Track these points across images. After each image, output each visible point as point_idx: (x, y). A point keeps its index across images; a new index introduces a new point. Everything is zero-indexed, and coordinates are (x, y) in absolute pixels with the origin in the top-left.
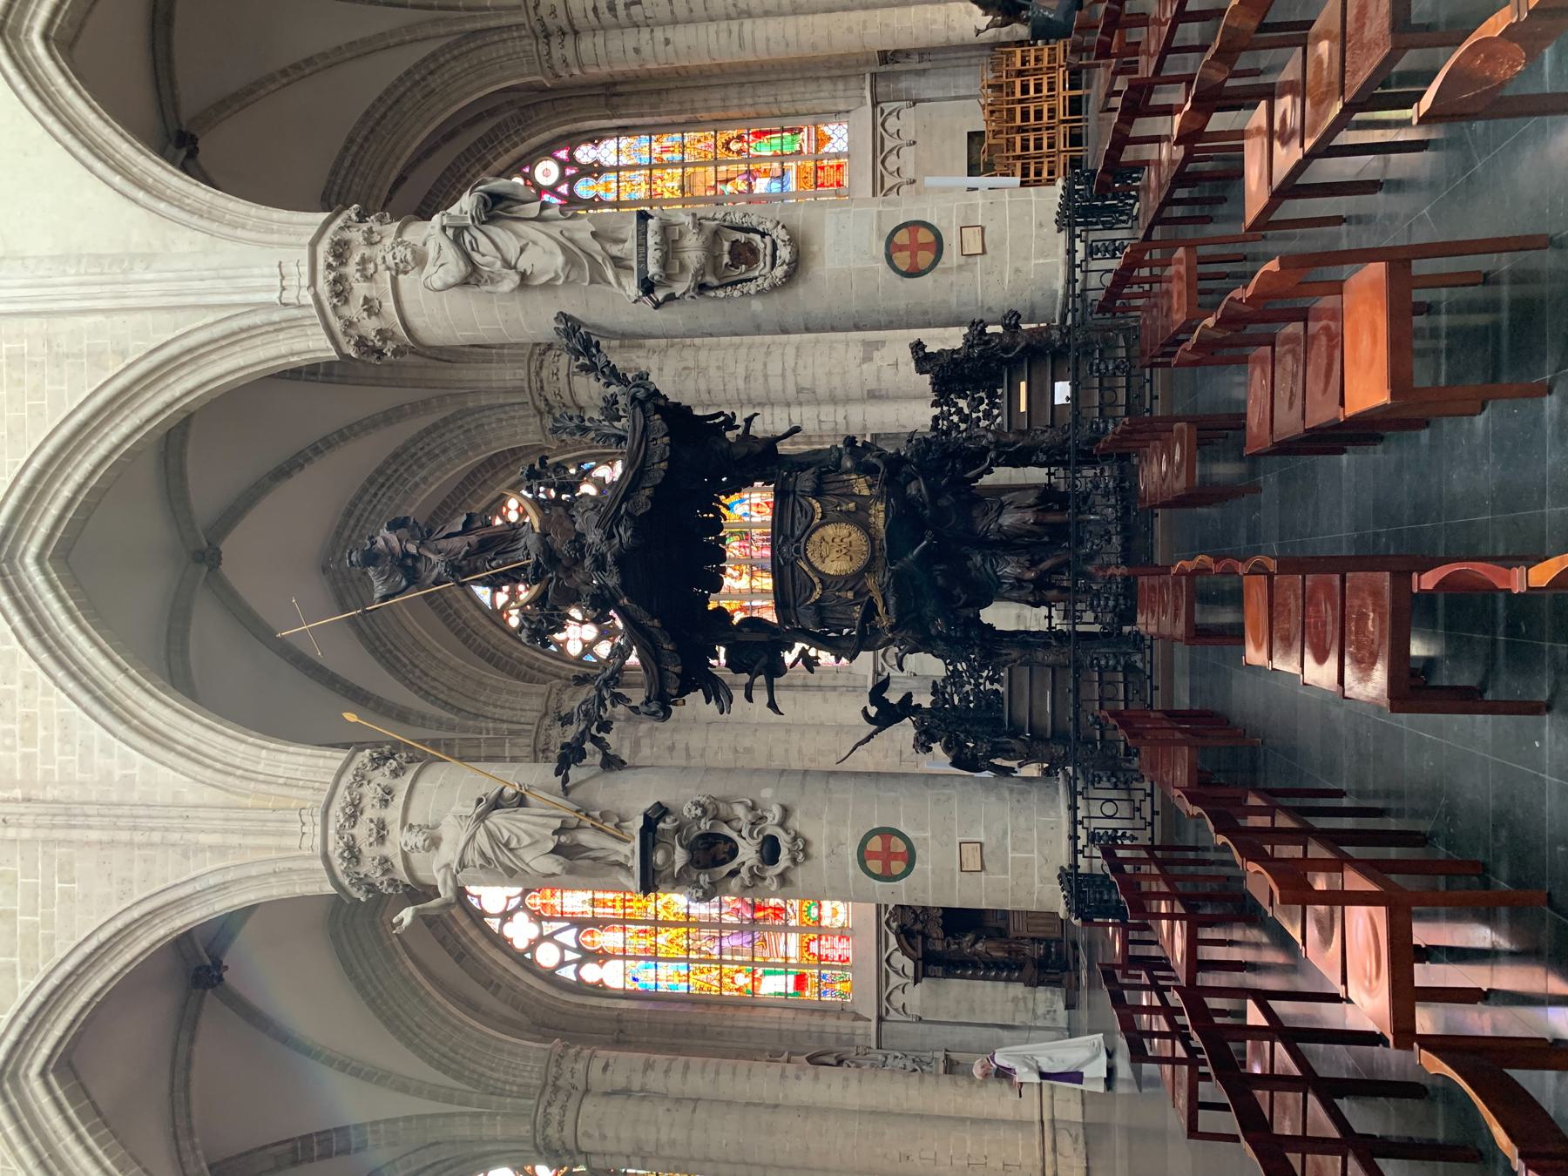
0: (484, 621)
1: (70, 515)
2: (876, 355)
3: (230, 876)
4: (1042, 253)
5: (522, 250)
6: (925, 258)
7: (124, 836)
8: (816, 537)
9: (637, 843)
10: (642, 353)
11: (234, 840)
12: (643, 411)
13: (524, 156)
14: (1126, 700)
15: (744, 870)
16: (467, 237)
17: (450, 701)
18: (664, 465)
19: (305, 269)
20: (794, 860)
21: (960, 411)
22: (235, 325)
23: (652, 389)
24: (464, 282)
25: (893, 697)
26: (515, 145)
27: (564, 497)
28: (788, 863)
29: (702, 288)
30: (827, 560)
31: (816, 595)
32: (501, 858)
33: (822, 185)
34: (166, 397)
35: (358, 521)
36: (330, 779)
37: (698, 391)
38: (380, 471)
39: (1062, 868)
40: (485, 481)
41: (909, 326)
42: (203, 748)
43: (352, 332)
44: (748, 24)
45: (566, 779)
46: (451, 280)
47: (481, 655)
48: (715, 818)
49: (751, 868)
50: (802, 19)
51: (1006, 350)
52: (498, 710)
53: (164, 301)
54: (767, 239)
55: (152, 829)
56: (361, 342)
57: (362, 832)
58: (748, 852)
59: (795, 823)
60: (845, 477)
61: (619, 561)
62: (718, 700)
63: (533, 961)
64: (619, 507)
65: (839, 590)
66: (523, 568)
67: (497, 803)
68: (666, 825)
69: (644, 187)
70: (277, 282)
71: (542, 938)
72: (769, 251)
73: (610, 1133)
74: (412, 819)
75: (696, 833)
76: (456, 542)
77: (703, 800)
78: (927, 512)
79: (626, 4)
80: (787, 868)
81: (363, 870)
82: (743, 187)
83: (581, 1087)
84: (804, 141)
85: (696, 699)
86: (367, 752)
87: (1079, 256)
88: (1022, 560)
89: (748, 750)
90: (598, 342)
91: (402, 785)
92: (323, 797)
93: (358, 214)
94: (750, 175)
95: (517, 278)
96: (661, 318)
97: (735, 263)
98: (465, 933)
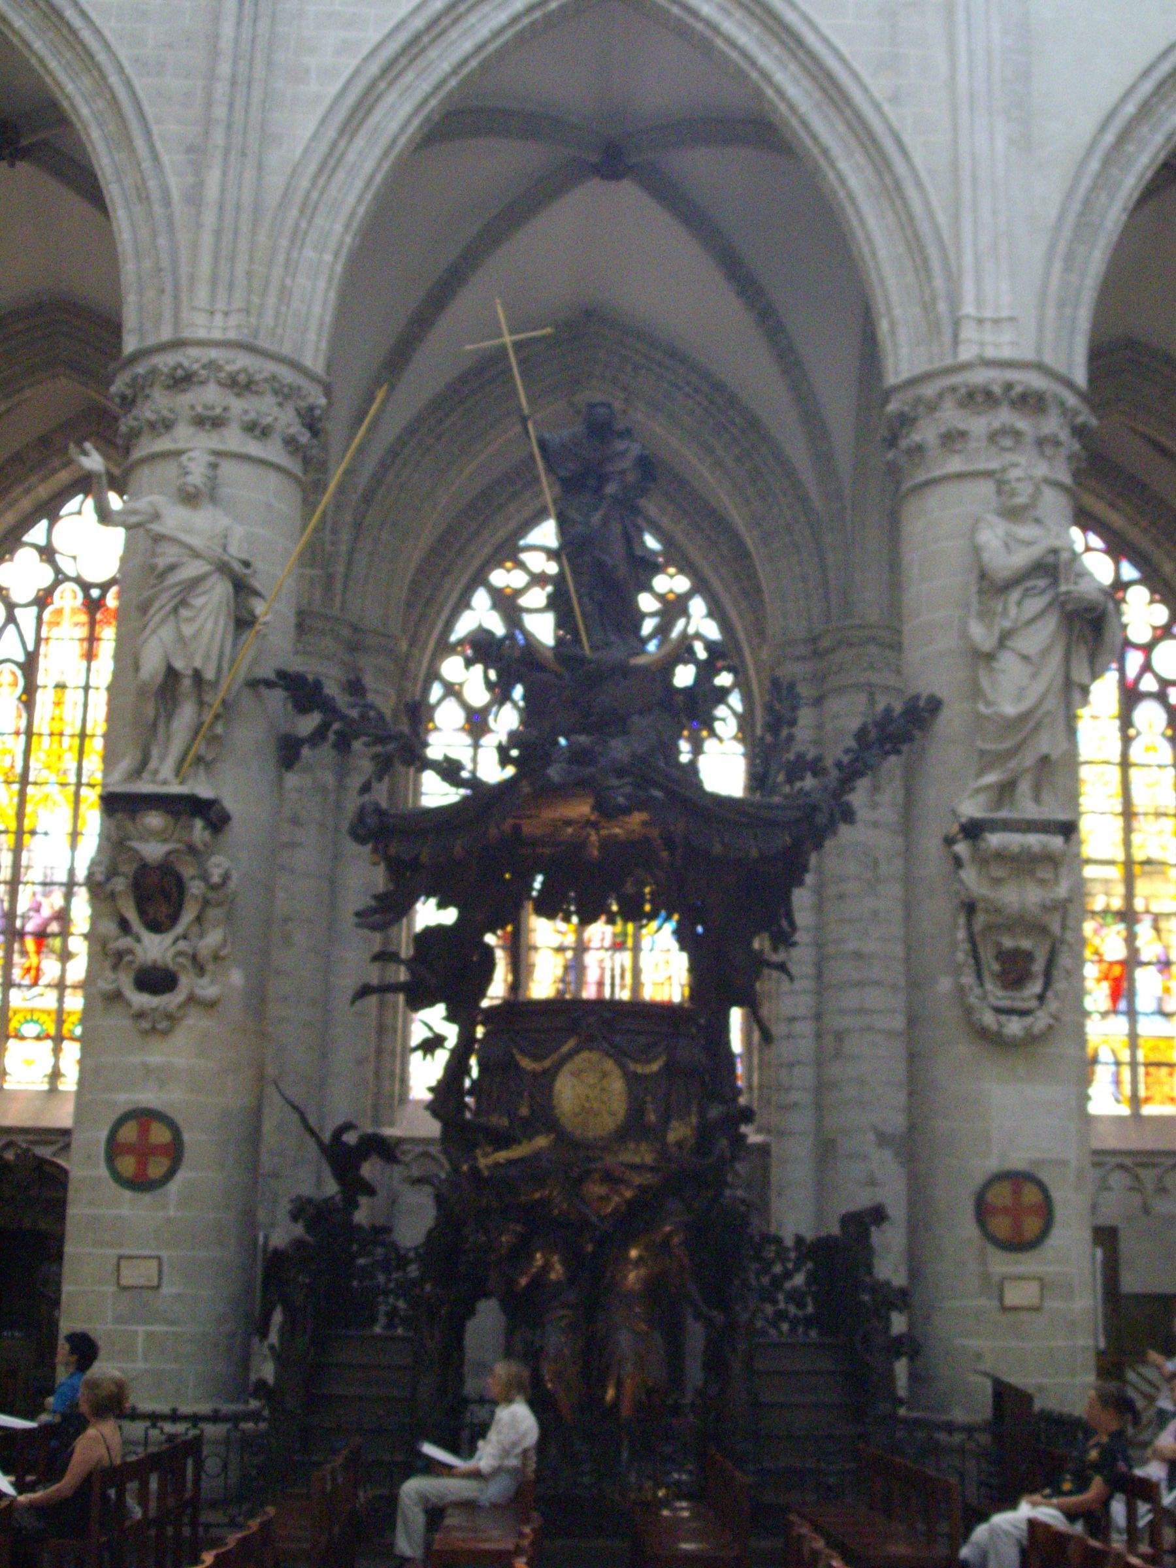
0: (501, 534)
2: (887, 1154)
3: (158, 209)
5: (1025, 658)
7: (224, 69)
8: (609, 1065)
9: (175, 789)
11: (209, 218)
19: (1006, 353)
20: (140, 1015)
21: (788, 1275)
24: (983, 576)
25: (369, 1169)
29: (970, 908)
30: (575, 1081)
31: (526, 1063)
32: (164, 598)
33: (1147, 1074)
34: (836, 150)
35: (660, 364)
36: (286, 350)
38: (733, 400)
41: (912, 1203)
42: (341, 175)
45: (269, 684)
46: (986, 556)
53: (965, 162)
55: (231, 106)
56: (905, 421)
57: (210, 395)
62: (372, 911)
64: (656, 784)
65: (531, 1096)
67: (242, 588)
68: (199, 831)
70: (988, 313)
71: (10, 607)
74: (228, 468)
75: (188, 871)
76: (619, 548)
77: (232, 885)
80: (128, 1004)
86: (323, 401)
89: (287, 940)
90: (898, 752)
91: (273, 451)
92: (263, 343)
96: (931, 845)
98: (27, 491)
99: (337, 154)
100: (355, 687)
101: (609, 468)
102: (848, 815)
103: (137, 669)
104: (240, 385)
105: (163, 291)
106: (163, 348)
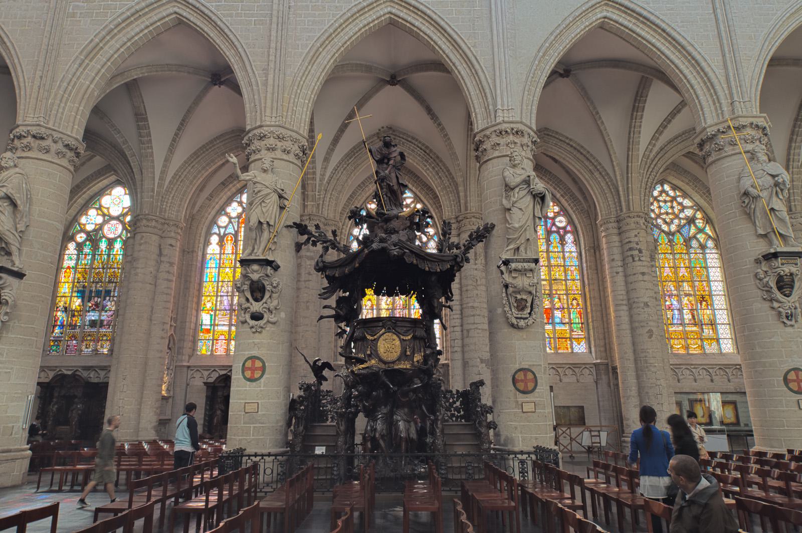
1: (408, 25)
2: (484, 365)
3: (255, 87)
4: (524, 439)
6: (521, 386)
8: (395, 337)
9: (262, 257)
14: (318, 479)
15: (248, 305)
16: (525, 186)
18: (427, 269)
20: (252, 327)
21: (454, 402)
22: (487, 91)
23: (461, 265)
24: (506, 185)
25: (326, 373)
26: (572, 208)
28: (251, 325)
29: (506, 286)
31: (369, 337)
37: (467, 286)
39: (245, 450)
43: (485, 139)
44: (625, 308)
45: (291, 227)
46: (507, 179)
47: (353, 193)
48: (272, 292)
49: (249, 308)
50: (628, 332)
51: (480, 423)
52: (328, 199)
54: (528, 316)
56: (481, 142)
57: (271, 141)
58: (256, 307)
59: (269, 327)
60: (422, 350)
61: (384, 250)
62: (324, 293)
63: (221, 215)
64: (408, 249)
69: (556, 263)
71: (230, 218)
72: (525, 316)
73: (142, 247)
75: (266, 283)
76: (395, 181)
77: (280, 287)
81: (255, 142)
82: (557, 306)
83: (163, 235)
84: (578, 333)
85: (326, 283)
87: (519, 456)
88: (384, 431)
89: (308, 308)
91: (291, 157)
92: (287, 126)
93: (535, 141)
94: (562, 309)
95: (508, 207)
97: (517, 300)
99: (308, 70)
101: (391, 156)
102: (467, 260)
104: (280, 138)
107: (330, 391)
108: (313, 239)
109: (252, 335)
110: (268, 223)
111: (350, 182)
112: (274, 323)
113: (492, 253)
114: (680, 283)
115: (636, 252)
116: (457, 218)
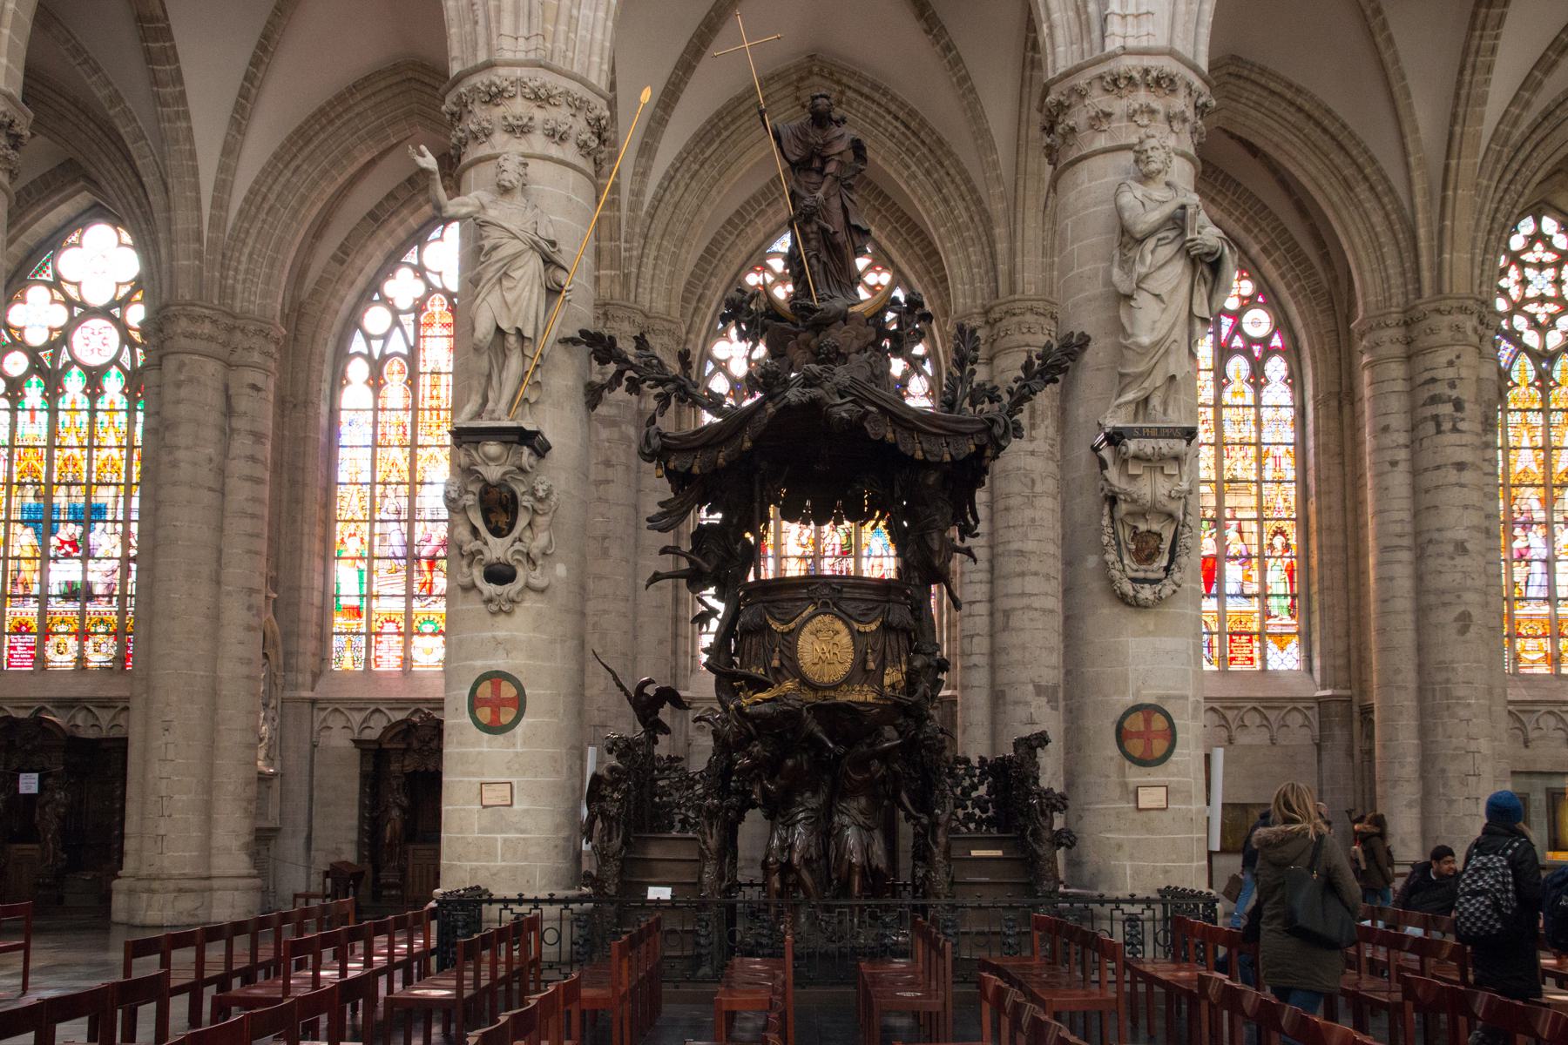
0: (752, 245)
8: (839, 625)
10: (1051, 431)
12: (980, 432)
13: (1276, 296)
17: (662, 205)
18: (919, 455)
23: (1003, 443)
26: (1289, 286)
27: (887, 343)
30: (813, 637)
31: (775, 626)
40: (912, 247)
47: (714, 241)
52: (651, 262)
60: (904, 658)
61: (815, 404)
64: (873, 404)
65: (781, 651)
66: (809, 295)
78: (865, 749)
79: (1437, 416)
88: (812, 850)
90: (1056, 381)
98: (402, 222)
100: (641, 342)
103: (473, 329)
105: (476, 23)
106: (477, 70)
107: (679, 759)
108: (629, 373)
109: (489, 619)
110: (519, 331)
111: (707, 212)
112: (542, 591)
113: (1081, 412)
114: (1556, 492)
115: (1446, 409)
116: (986, 312)
